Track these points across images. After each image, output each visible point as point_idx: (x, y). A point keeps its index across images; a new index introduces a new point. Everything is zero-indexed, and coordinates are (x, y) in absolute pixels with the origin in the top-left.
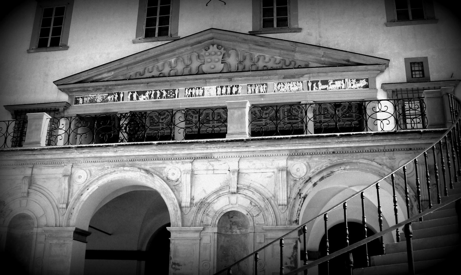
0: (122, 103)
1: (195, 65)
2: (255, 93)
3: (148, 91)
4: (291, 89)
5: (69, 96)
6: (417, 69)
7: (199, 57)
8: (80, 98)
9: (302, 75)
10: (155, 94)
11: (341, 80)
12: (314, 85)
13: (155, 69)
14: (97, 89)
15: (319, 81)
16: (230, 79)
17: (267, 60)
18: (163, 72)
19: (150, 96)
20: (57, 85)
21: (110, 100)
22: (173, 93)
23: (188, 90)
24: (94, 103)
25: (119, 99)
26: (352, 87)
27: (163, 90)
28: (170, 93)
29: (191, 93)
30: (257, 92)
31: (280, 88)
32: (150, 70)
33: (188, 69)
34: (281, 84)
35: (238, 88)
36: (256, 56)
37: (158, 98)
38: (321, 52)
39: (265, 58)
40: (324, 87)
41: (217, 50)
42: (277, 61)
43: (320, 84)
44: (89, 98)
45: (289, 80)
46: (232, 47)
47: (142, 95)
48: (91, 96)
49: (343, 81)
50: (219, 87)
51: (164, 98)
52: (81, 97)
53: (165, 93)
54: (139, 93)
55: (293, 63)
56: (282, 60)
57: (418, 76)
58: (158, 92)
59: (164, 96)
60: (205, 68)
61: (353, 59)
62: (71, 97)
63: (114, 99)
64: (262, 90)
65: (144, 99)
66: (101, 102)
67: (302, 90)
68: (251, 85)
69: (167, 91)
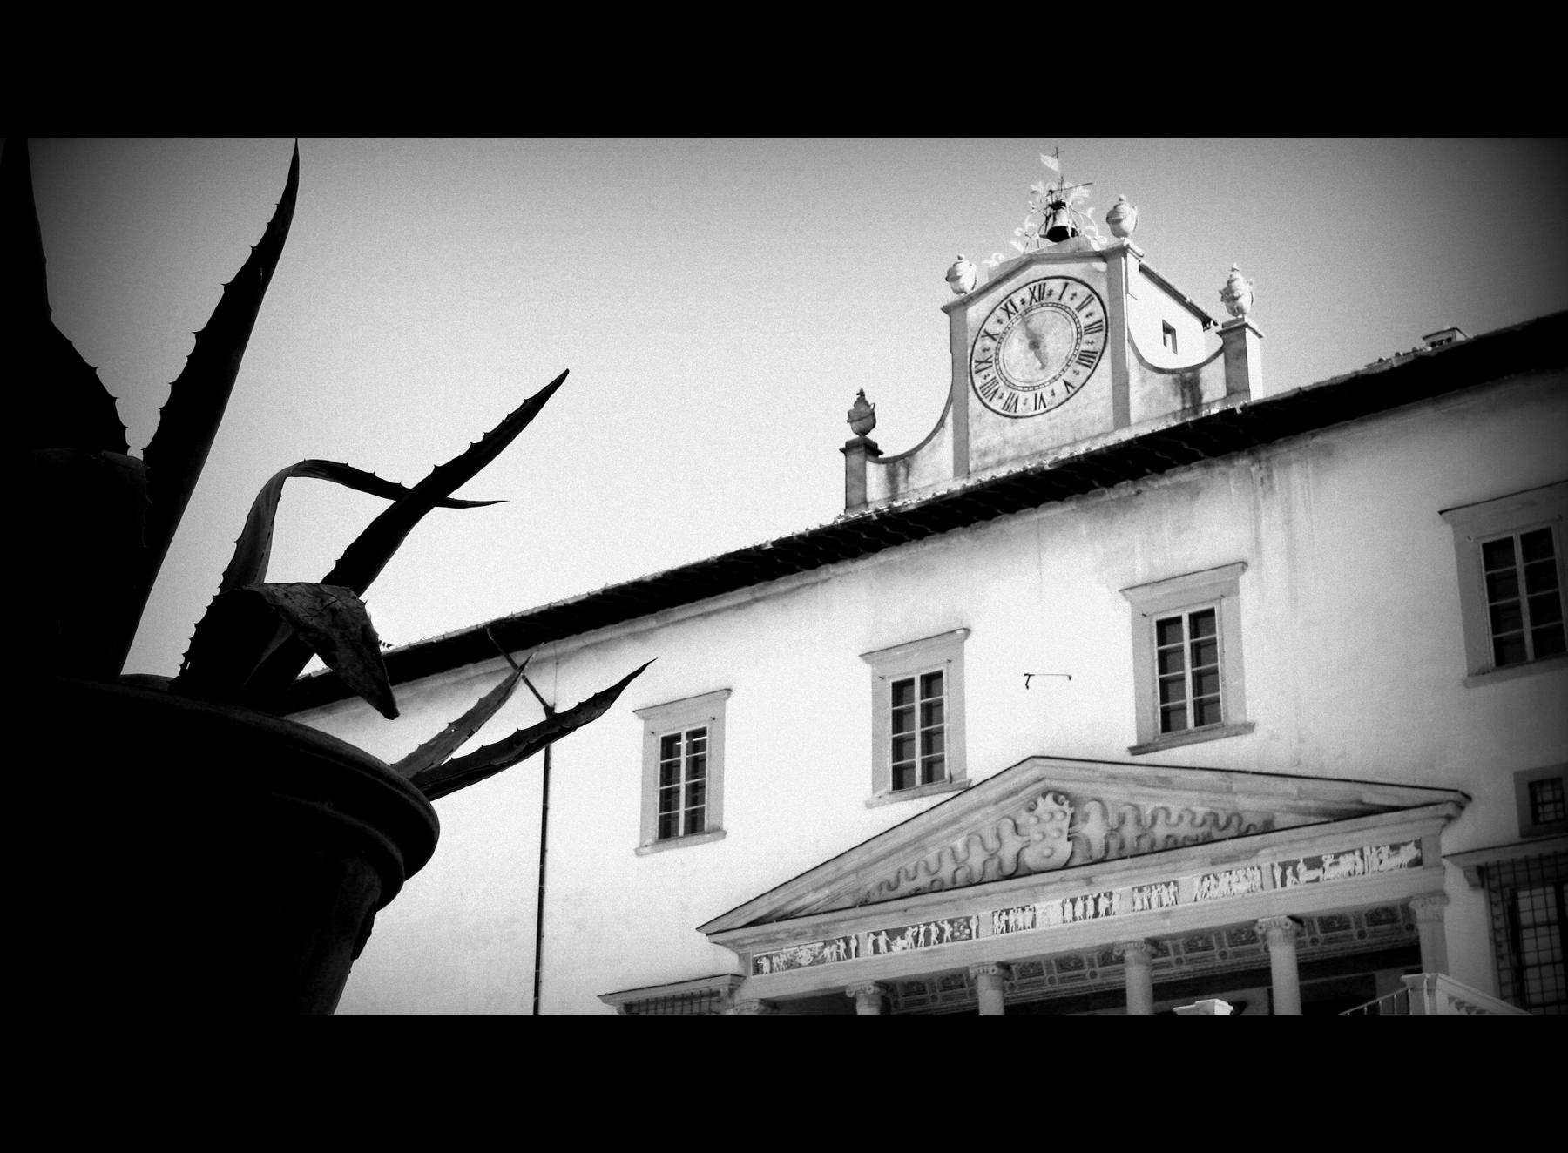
0: (857, 964)
1: (1008, 854)
2: (1150, 907)
3: (910, 928)
4: (1234, 890)
5: (739, 955)
6: (1548, 796)
7: (1016, 828)
8: (765, 958)
9: (1255, 852)
10: (928, 934)
11: (1353, 852)
12: (1289, 871)
13: (921, 872)
14: (798, 935)
15: (1298, 862)
16: (1088, 881)
17: (1174, 819)
18: (940, 875)
19: (916, 938)
20: (708, 935)
21: (829, 956)
22: (965, 928)
23: (1000, 915)
24: (795, 967)
25: (847, 951)
26: (1382, 867)
27: (943, 923)
28: (959, 927)
29: (1007, 922)
30: (1154, 905)
31: (1209, 889)
32: (911, 874)
33: (996, 861)
34: (1209, 879)
35: (1110, 899)
36: (1148, 812)
37: (935, 943)
38: (1291, 786)
39: (1168, 816)
40: (1314, 874)
41: (1055, 807)
42: (1199, 821)
43: (1301, 867)
44: (783, 958)
45: (1226, 867)
46: (1090, 794)
47: (899, 938)
48: (788, 951)
49: (1358, 853)
50: (1068, 901)
51: (948, 941)
52: (767, 957)
53: (948, 928)
54: (893, 934)
55: (1235, 821)
56: (1211, 814)
57: (1551, 817)
58: (933, 927)
59: (947, 939)
60: (1031, 858)
61: (1372, 797)
62: (744, 958)
63: (838, 953)
64: (1165, 901)
65: (904, 949)
66: (810, 965)
67: (1260, 890)
68: (1140, 890)
69: (951, 922)
